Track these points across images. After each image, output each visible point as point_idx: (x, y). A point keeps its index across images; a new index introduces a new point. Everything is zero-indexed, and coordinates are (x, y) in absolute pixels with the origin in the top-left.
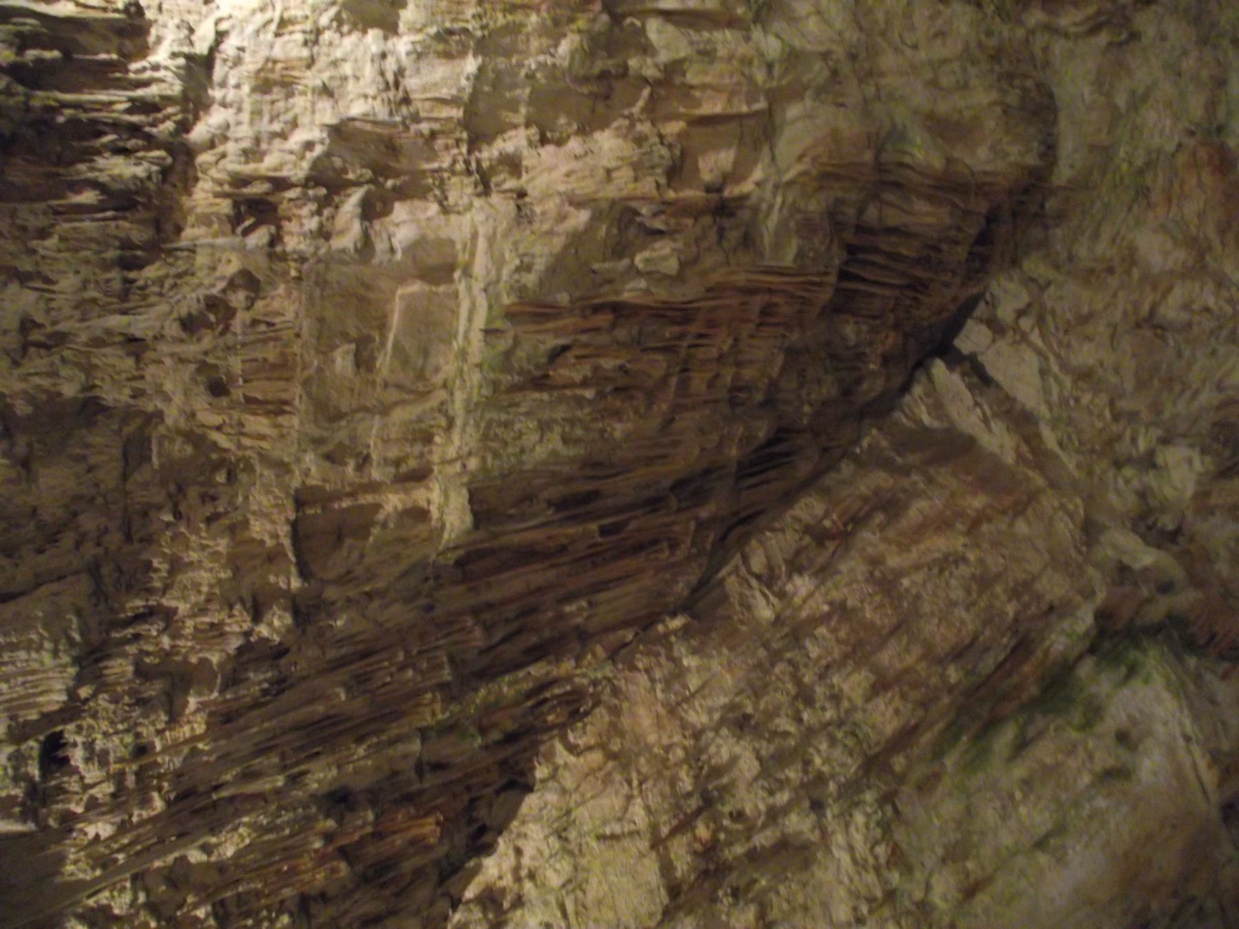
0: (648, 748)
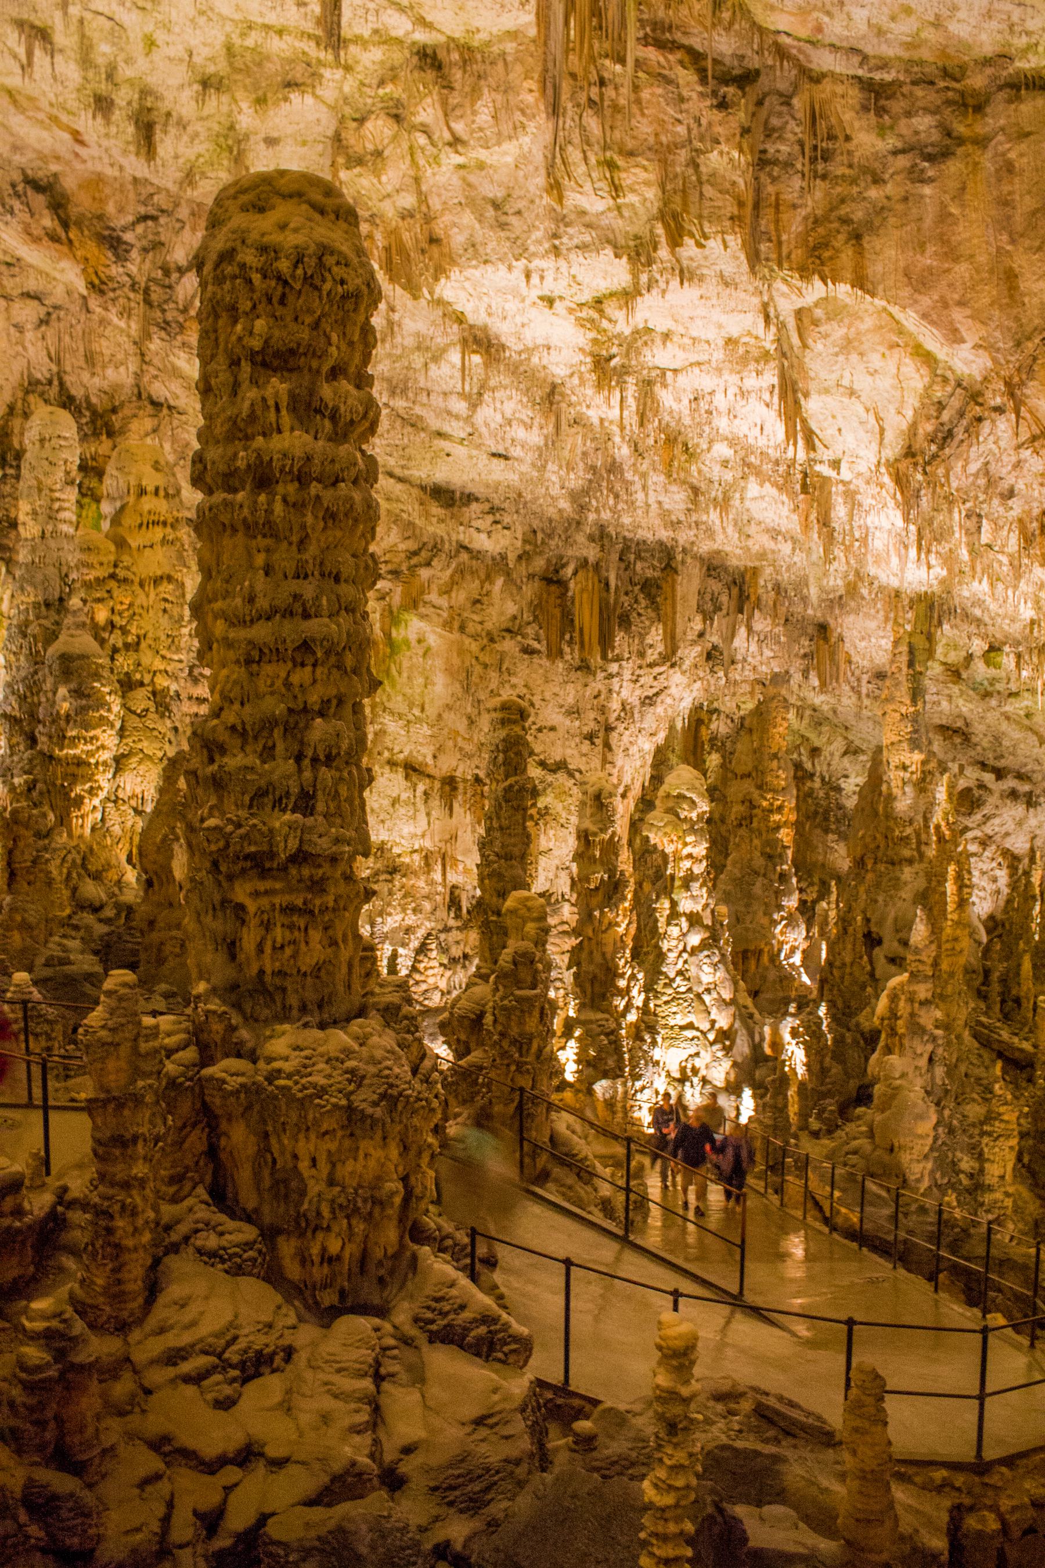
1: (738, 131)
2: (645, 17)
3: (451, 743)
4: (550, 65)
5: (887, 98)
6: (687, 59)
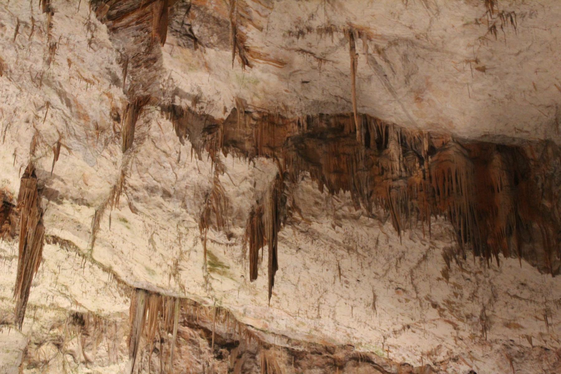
1: (227, 370)
2: (185, 313)
4: (134, 333)
5: (300, 359)
6: (203, 334)
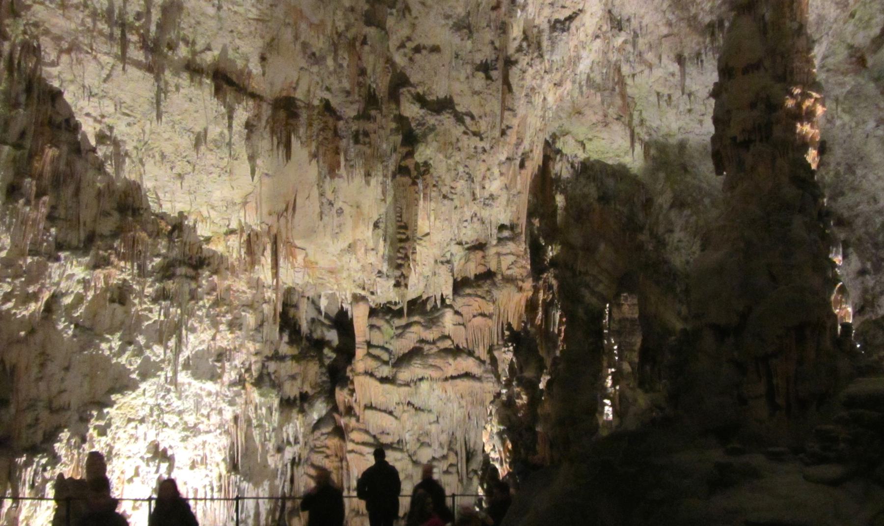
0: (76, 30)
3: (287, 35)
